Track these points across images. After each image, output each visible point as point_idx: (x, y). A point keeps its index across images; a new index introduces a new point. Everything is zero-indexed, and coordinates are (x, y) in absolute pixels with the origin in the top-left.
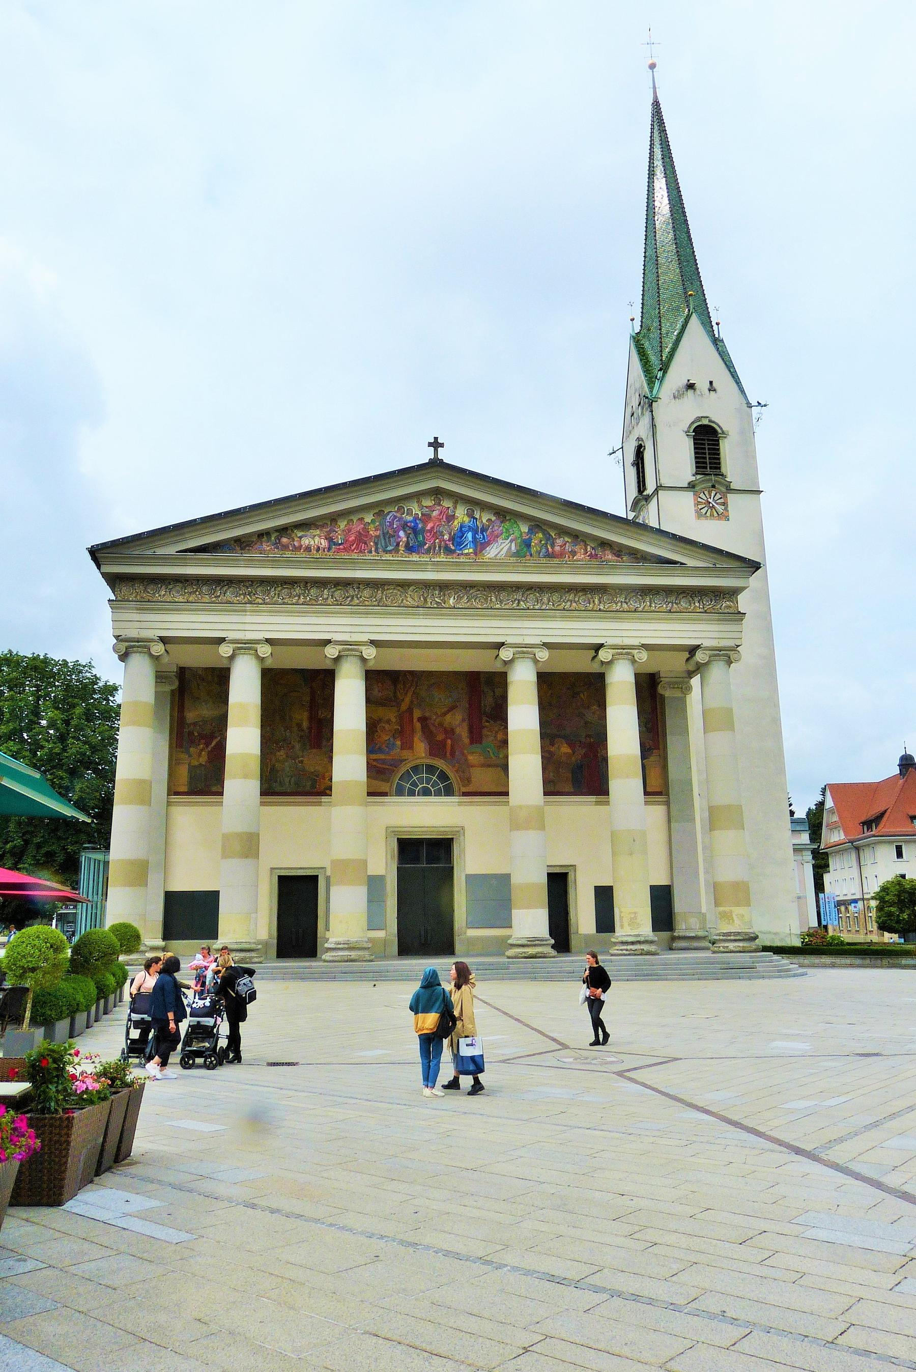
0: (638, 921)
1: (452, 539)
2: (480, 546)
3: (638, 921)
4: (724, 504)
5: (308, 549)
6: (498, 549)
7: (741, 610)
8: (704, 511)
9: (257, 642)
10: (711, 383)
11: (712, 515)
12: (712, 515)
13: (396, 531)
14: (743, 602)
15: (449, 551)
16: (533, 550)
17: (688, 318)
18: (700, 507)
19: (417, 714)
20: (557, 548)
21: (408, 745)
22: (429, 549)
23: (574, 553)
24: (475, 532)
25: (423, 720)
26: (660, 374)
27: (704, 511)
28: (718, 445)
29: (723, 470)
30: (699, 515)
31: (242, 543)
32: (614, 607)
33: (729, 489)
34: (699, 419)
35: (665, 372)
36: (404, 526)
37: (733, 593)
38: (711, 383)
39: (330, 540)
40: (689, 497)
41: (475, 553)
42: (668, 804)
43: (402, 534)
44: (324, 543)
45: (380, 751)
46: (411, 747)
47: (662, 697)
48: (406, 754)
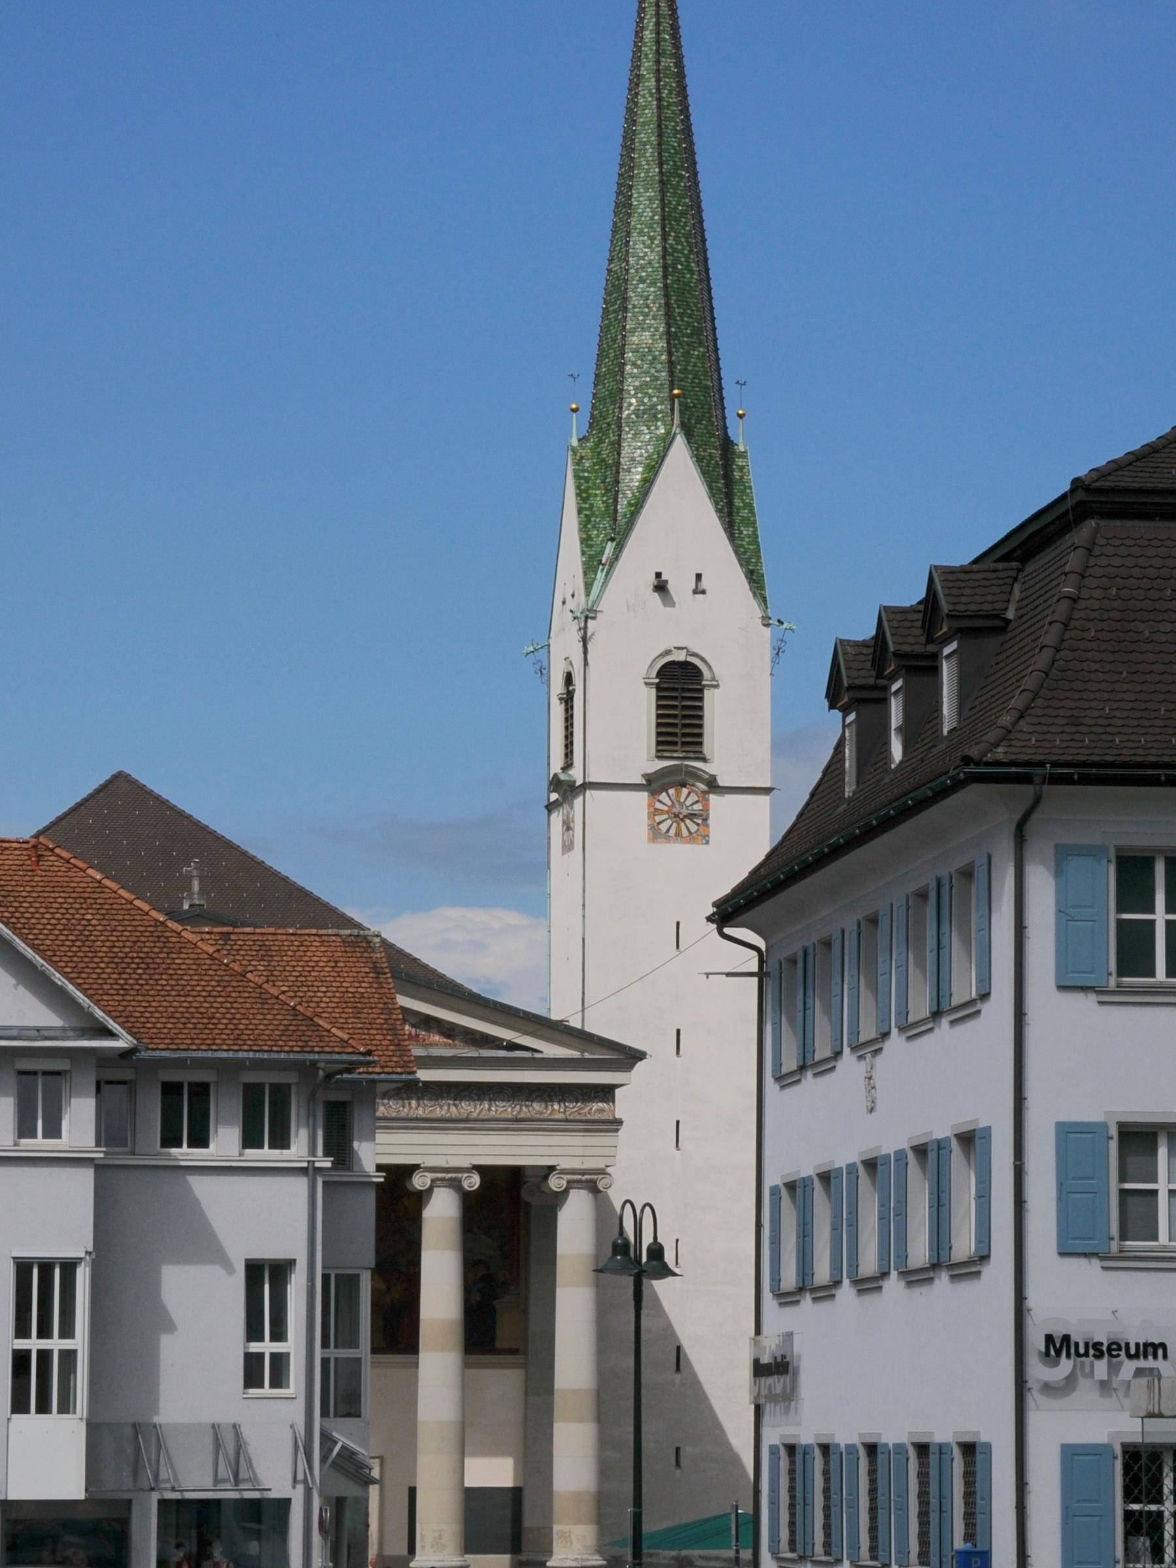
0: (443, 1541)
3: (443, 1541)
7: (617, 1116)
8: (664, 827)
10: (699, 577)
11: (678, 834)
12: (678, 834)
14: (623, 1104)
17: (666, 443)
18: (658, 819)
26: (610, 547)
27: (664, 827)
28: (701, 699)
29: (706, 749)
30: (656, 834)
33: (713, 785)
34: (668, 652)
35: (619, 549)
37: (606, 1093)
38: (699, 577)
40: (644, 795)
42: (525, 1366)
47: (528, 1204)
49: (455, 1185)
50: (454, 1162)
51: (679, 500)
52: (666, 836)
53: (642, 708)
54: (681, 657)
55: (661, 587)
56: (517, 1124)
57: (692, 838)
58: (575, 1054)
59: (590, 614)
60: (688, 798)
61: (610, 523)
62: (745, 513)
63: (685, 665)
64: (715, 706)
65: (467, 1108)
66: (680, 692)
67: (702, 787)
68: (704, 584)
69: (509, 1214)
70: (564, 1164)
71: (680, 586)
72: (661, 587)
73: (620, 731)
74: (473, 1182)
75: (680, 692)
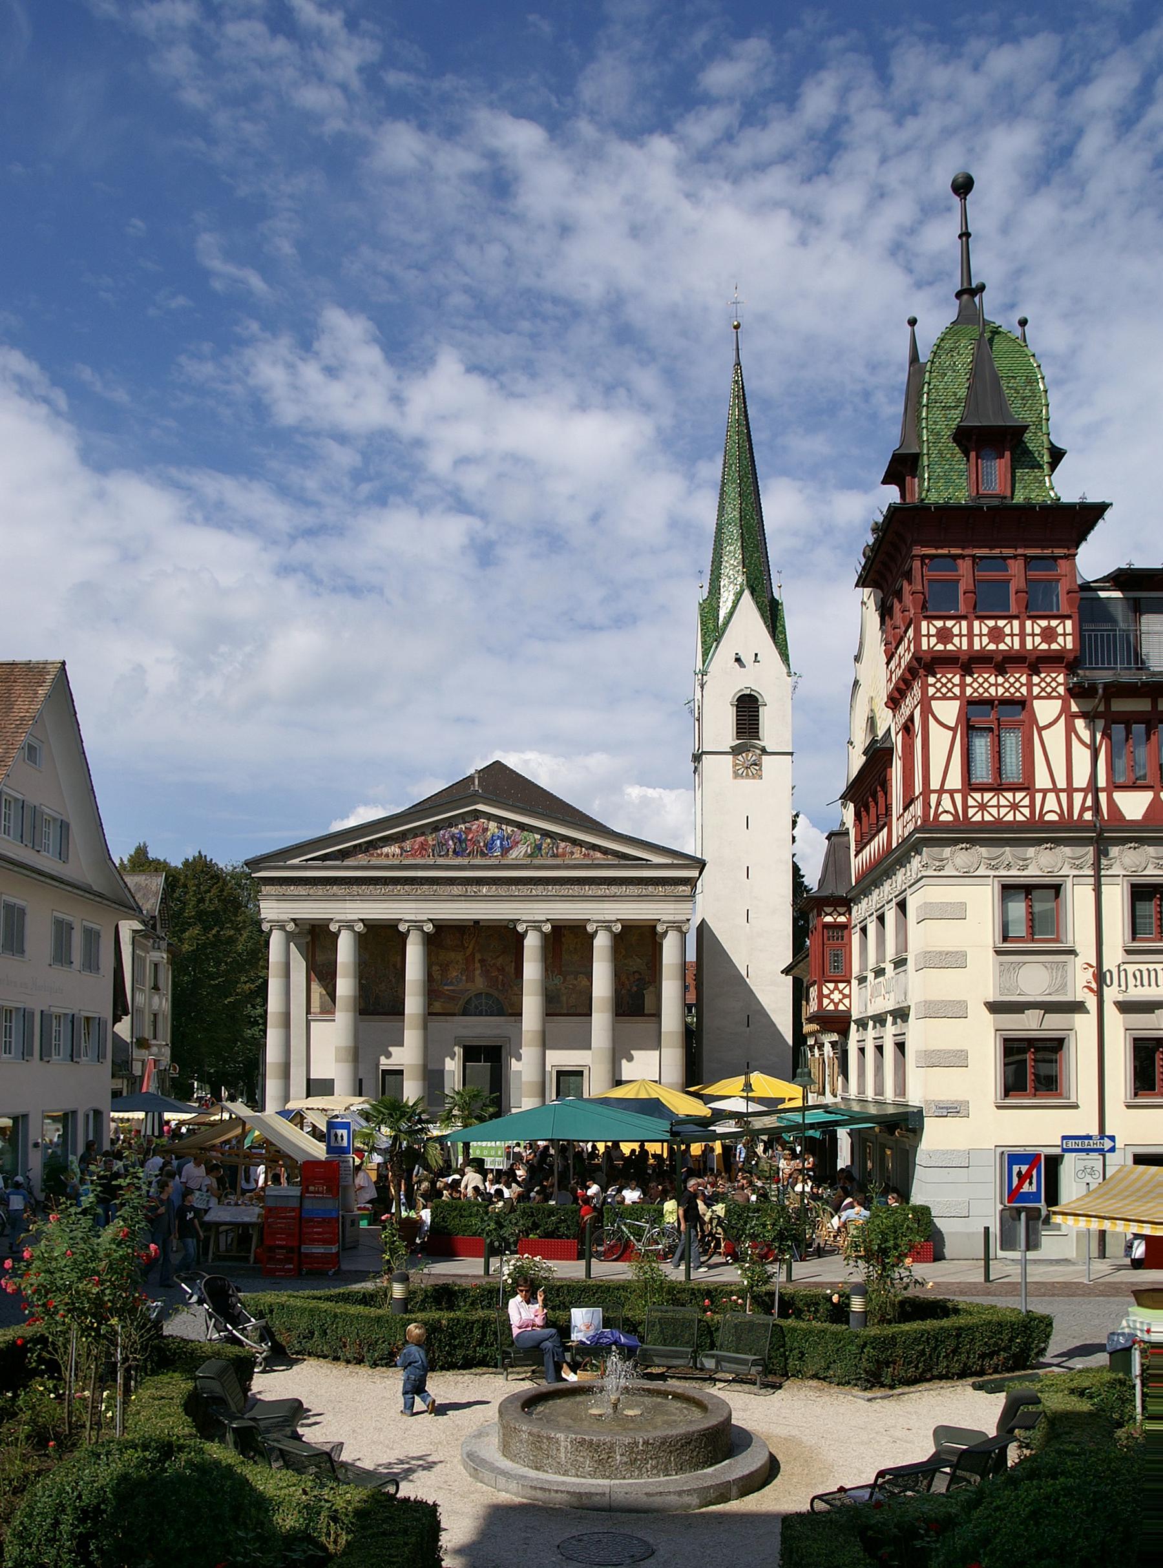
1: (486, 845)
2: (505, 851)
4: (760, 765)
5: (387, 855)
6: (518, 853)
9: (354, 921)
11: (747, 775)
12: (747, 775)
13: (447, 841)
15: (483, 855)
16: (543, 852)
19: (478, 956)
20: (560, 850)
21: (471, 979)
22: (469, 854)
23: (572, 853)
24: (502, 840)
25: (482, 961)
30: (736, 775)
31: (344, 854)
32: (599, 893)
33: (764, 751)
36: (453, 837)
39: (401, 848)
41: (502, 855)
43: (451, 842)
44: (398, 851)
45: (451, 984)
46: (473, 981)
48: (469, 985)
49: (608, 929)
50: (608, 918)
51: (746, 627)
52: (741, 776)
53: (728, 717)
54: (748, 692)
55: (738, 660)
56: (640, 898)
57: (754, 777)
58: (669, 861)
59: (704, 673)
60: (751, 757)
61: (712, 631)
62: (780, 629)
63: (750, 696)
64: (766, 717)
65: (614, 890)
66: (748, 709)
67: (758, 752)
68: (759, 658)
69: (638, 945)
70: (664, 918)
71: (747, 659)
72: (738, 660)
73: (721, 727)
74: (618, 928)
75: (748, 709)
